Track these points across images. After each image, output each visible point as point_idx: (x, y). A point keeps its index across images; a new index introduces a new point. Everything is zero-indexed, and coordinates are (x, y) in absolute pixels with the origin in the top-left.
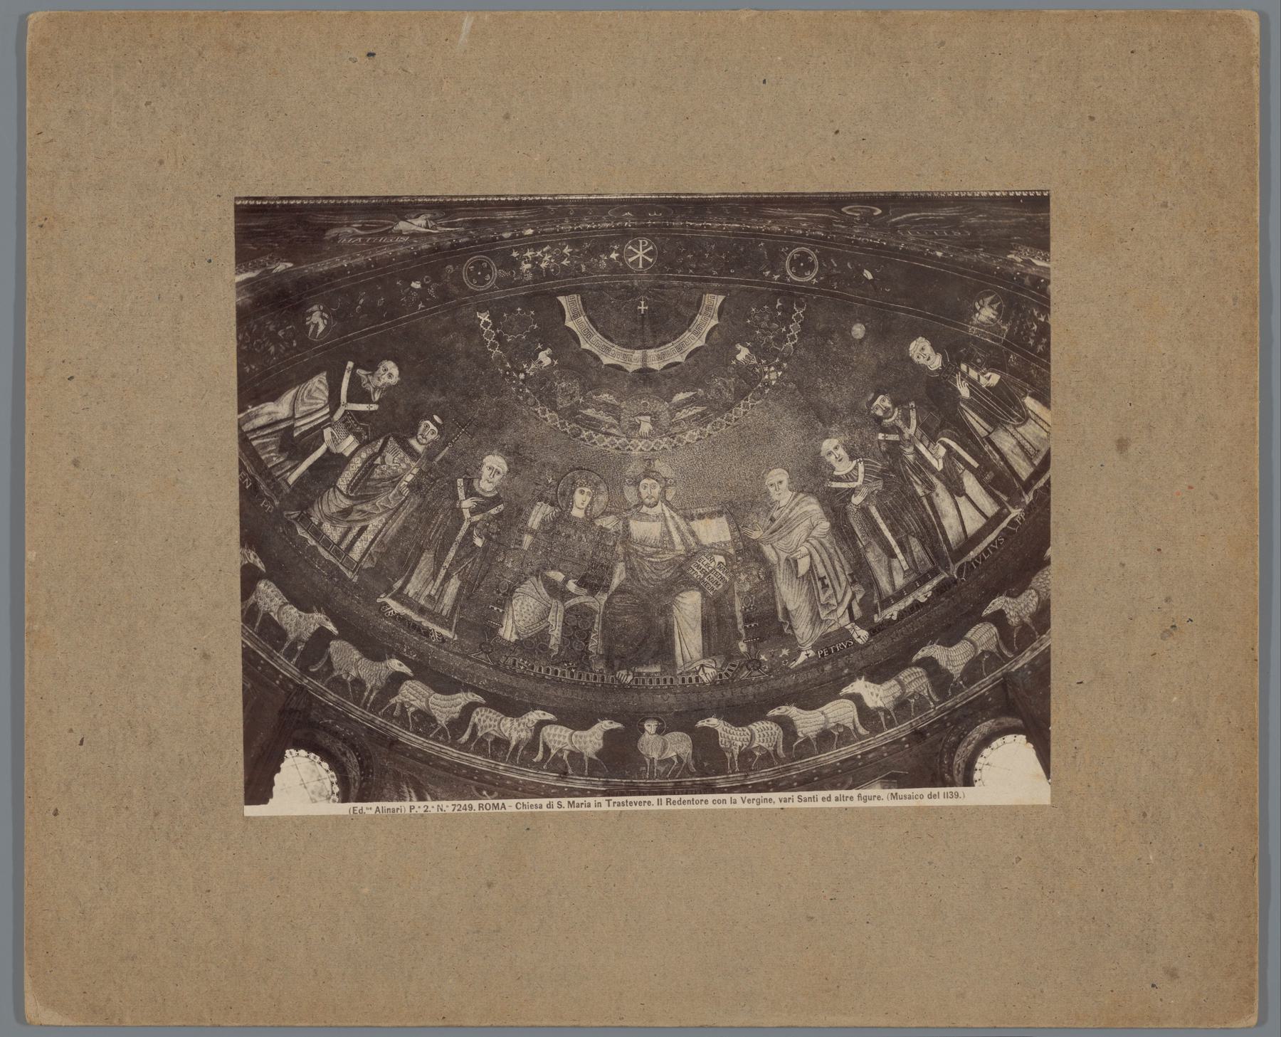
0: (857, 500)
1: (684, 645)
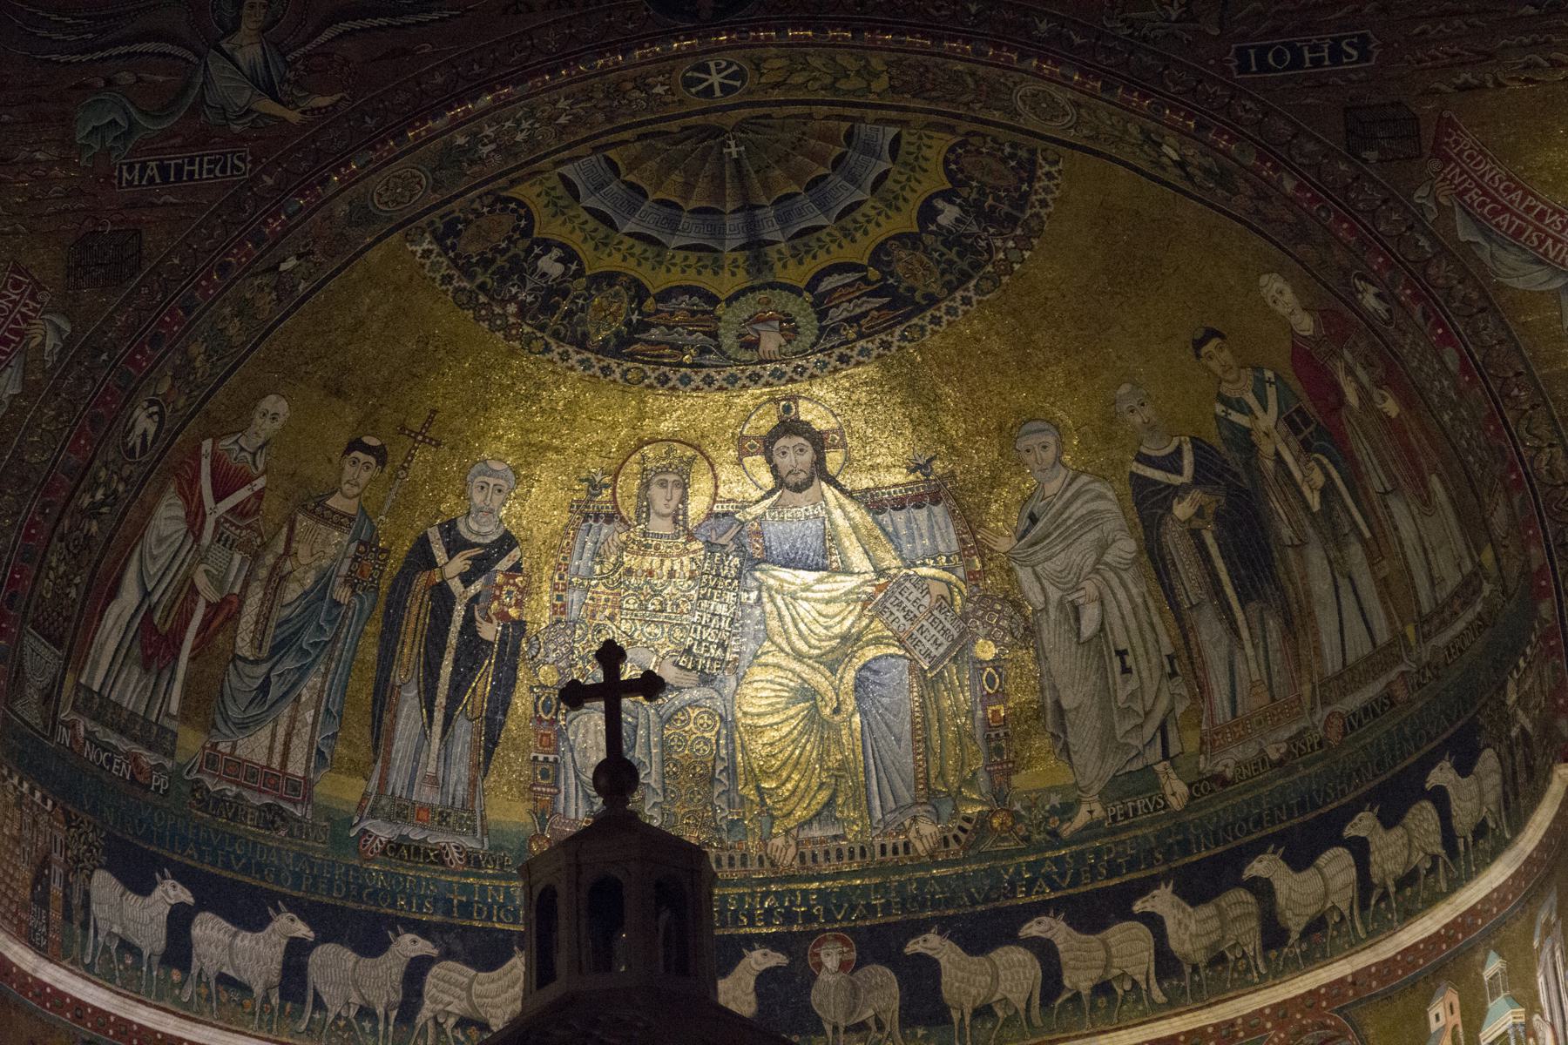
1: (882, 774)
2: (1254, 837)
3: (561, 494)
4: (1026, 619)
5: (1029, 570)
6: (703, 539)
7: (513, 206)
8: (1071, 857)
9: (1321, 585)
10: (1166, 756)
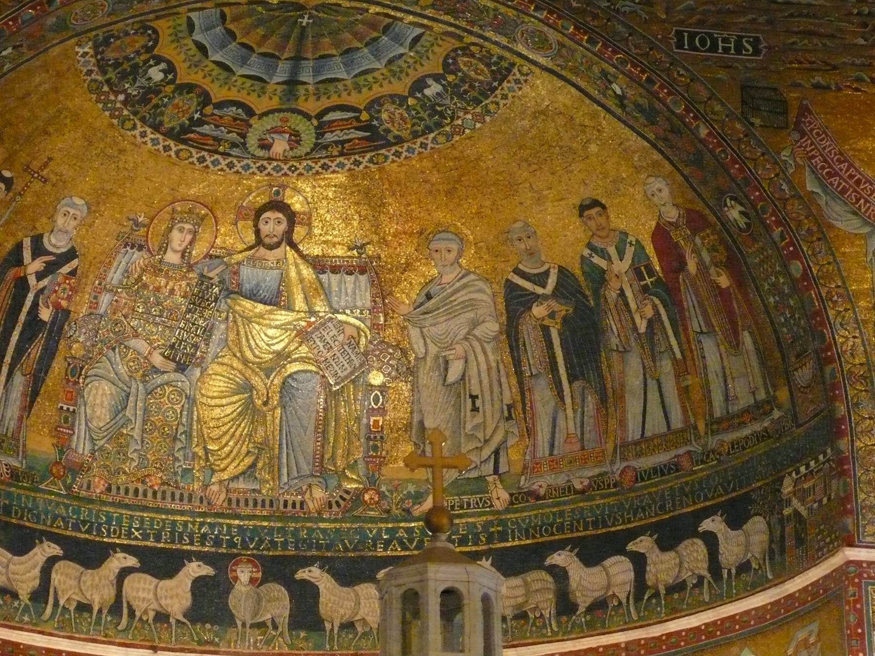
0: (538, 310)
1: (291, 452)
2: (557, 537)
3: (115, 226)
4: (409, 362)
5: (418, 330)
6: (198, 271)
7: (150, 32)
8: (418, 529)
9: (634, 381)
10: (496, 471)
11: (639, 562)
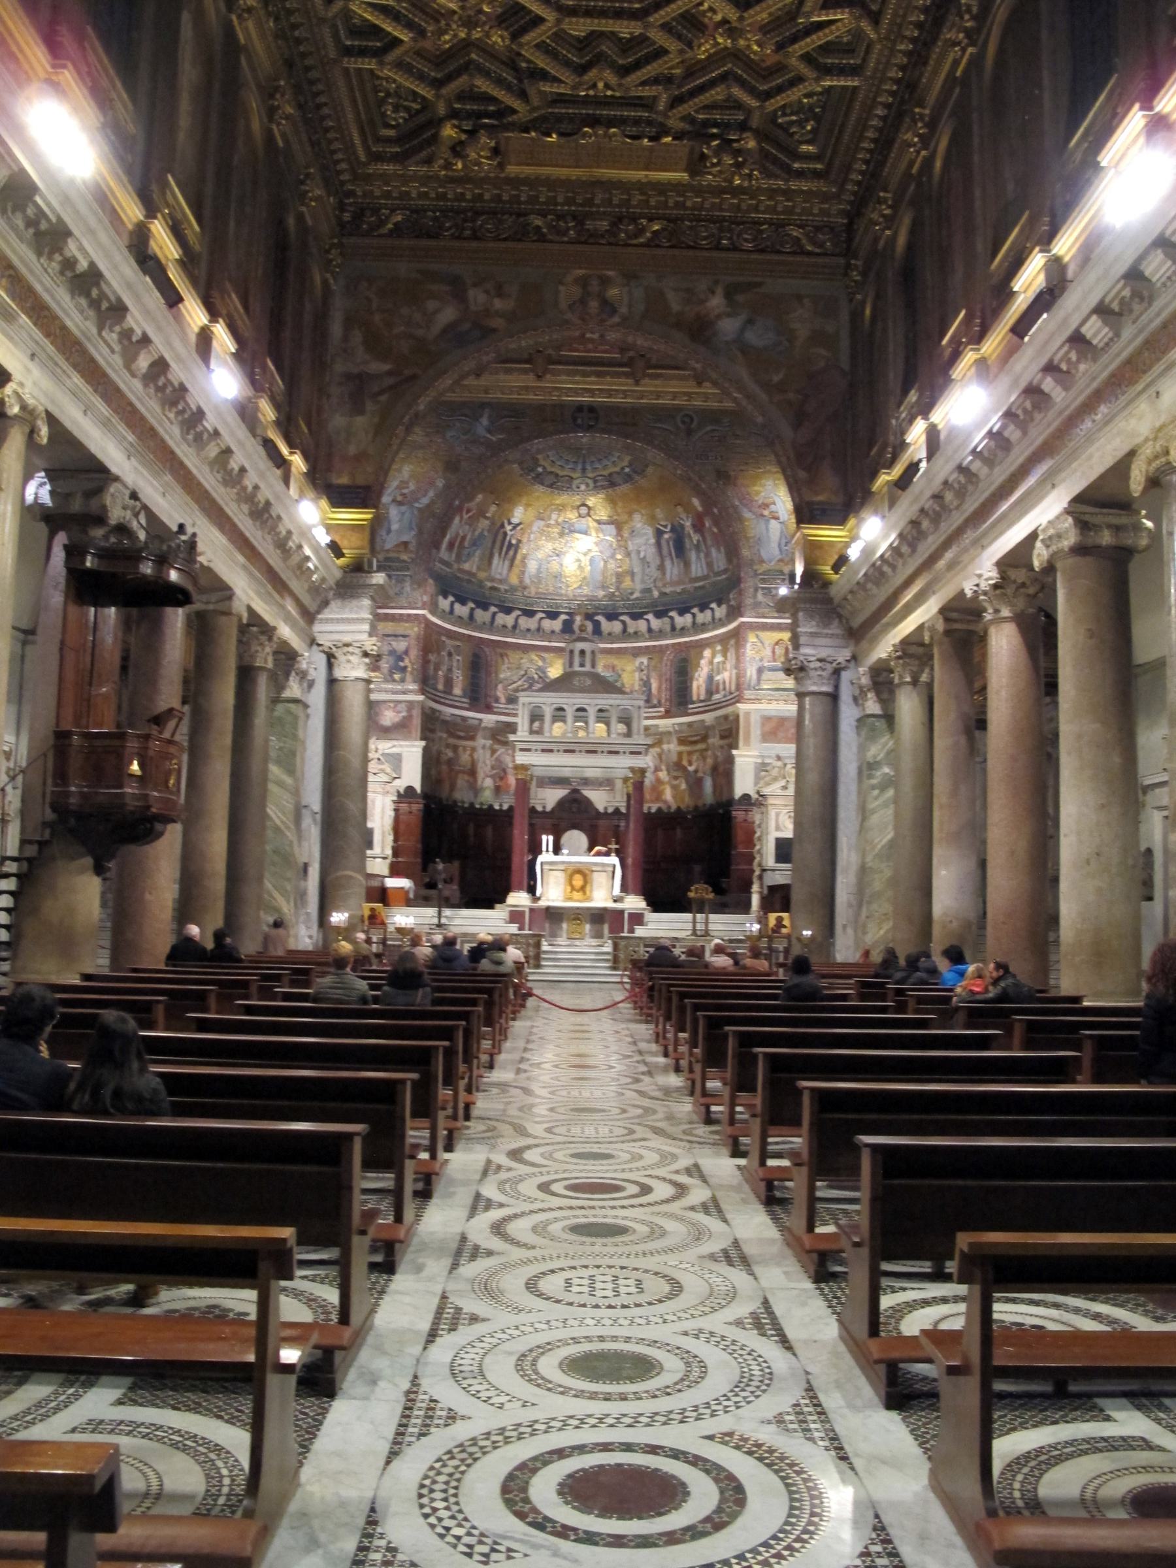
0: (666, 536)
11: (694, 615)
